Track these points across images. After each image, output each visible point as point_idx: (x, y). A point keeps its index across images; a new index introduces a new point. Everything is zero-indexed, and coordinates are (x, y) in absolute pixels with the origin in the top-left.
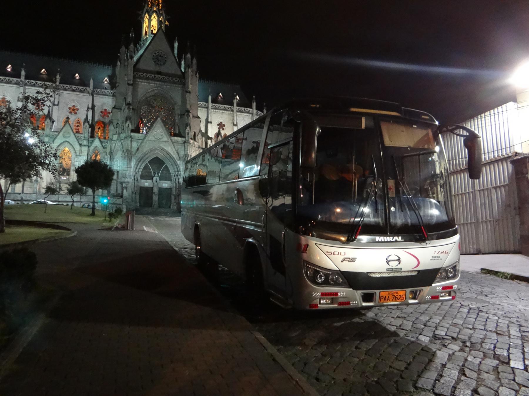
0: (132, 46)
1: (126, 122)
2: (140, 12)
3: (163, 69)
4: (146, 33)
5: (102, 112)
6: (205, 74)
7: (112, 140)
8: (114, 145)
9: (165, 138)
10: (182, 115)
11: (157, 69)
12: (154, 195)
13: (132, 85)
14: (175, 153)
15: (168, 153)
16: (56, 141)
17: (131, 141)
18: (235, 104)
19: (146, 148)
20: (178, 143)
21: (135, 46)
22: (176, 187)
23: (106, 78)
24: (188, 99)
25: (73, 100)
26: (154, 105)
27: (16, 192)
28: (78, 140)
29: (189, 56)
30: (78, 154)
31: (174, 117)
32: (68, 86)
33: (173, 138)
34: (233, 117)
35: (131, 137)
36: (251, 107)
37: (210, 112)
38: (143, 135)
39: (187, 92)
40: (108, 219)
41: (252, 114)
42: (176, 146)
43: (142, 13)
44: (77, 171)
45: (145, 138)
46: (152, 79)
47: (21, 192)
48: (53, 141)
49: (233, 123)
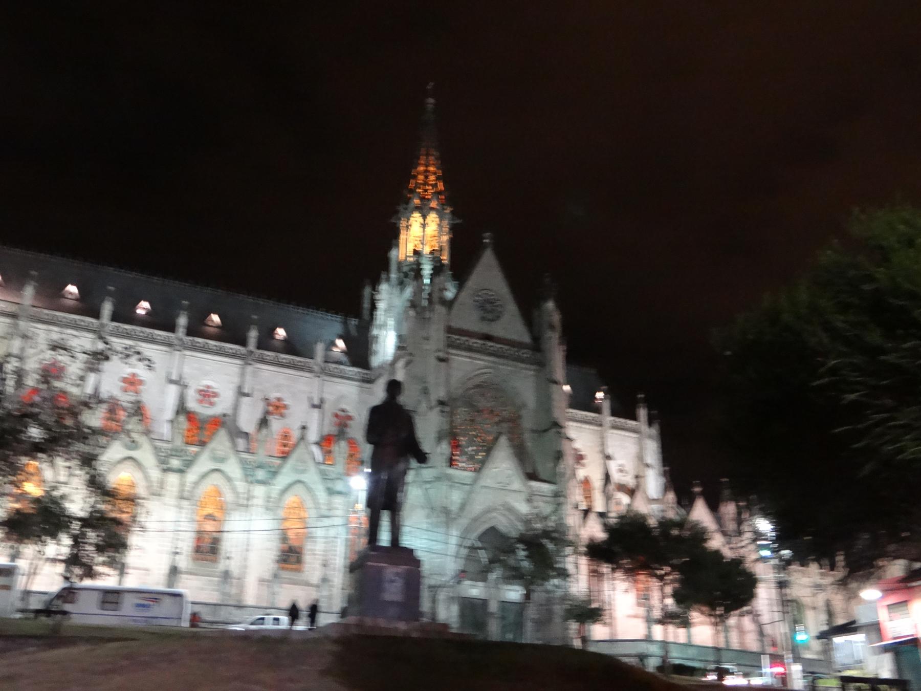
3: (497, 329)
9: (518, 483)
10: (540, 432)
11: (484, 328)
19: (480, 503)
25: (278, 387)
31: (522, 434)
35: (449, 478)
36: (634, 418)
45: (475, 481)
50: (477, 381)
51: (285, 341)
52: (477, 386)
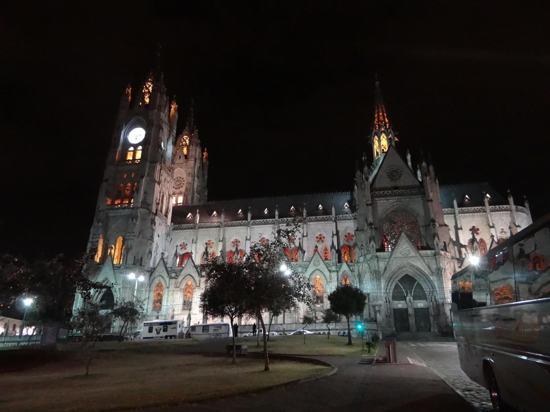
0: (366, 168)
1: (370, 242)
2: (369, 137)
3: (400, 183)
4: (377, 153)
5: (345, 236)
6: (445, 179)
7: (358, 262)
8: (361, 267)
9: (413, 254)
10: (427, 226)
11: (394, 184)
12: (409, 317)
13: (371, 205)
14: (427, 267)
15: (418, 269)
16: (308, 270)
17: (378, 261)
18: (487, 204)
19: (394, 265)
20: (427, 256)
21: (369, 168)
22: (433, 307)
23: (346, 204)
24: (430, 208)
26: (395, 221)
27: (279, 323)
28: (327, 267)
29: (424, 164)
30: (328, 278)
32: (314, 217)
33: (421, 252)
34: (487, 218)
35: (377, 257)
36: (508, 203)
37: (457, 217)
38: (389, 253)
39: (428, 201)
40: (365, 348)
41: (510, 210)
42: (426, 260)
43: (371, 136)
44: (330, 298)
45: (391, 256)
46: (390, 195)
47: (282, 323)
48: (306, 271)
49: (489, 225)
50: (392, 210)
51: (323, 209)
52: (394, 211)
